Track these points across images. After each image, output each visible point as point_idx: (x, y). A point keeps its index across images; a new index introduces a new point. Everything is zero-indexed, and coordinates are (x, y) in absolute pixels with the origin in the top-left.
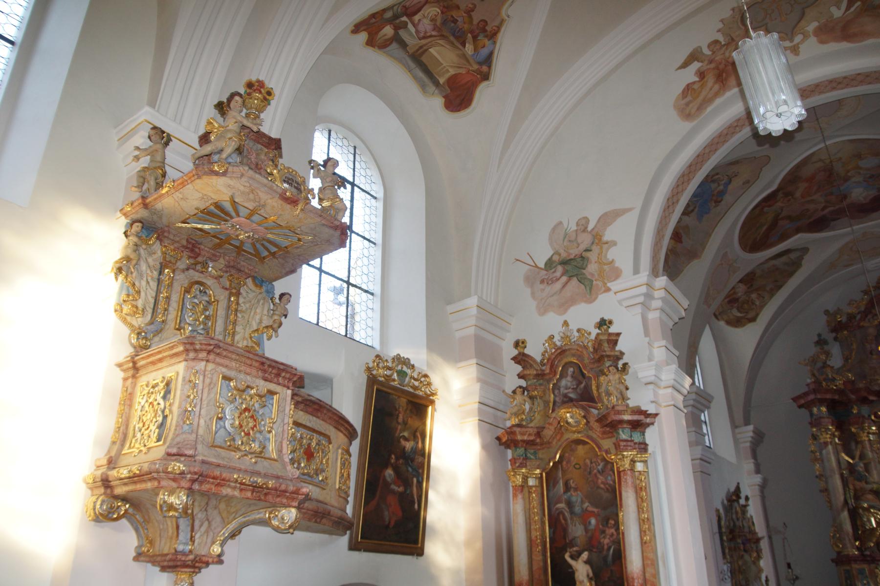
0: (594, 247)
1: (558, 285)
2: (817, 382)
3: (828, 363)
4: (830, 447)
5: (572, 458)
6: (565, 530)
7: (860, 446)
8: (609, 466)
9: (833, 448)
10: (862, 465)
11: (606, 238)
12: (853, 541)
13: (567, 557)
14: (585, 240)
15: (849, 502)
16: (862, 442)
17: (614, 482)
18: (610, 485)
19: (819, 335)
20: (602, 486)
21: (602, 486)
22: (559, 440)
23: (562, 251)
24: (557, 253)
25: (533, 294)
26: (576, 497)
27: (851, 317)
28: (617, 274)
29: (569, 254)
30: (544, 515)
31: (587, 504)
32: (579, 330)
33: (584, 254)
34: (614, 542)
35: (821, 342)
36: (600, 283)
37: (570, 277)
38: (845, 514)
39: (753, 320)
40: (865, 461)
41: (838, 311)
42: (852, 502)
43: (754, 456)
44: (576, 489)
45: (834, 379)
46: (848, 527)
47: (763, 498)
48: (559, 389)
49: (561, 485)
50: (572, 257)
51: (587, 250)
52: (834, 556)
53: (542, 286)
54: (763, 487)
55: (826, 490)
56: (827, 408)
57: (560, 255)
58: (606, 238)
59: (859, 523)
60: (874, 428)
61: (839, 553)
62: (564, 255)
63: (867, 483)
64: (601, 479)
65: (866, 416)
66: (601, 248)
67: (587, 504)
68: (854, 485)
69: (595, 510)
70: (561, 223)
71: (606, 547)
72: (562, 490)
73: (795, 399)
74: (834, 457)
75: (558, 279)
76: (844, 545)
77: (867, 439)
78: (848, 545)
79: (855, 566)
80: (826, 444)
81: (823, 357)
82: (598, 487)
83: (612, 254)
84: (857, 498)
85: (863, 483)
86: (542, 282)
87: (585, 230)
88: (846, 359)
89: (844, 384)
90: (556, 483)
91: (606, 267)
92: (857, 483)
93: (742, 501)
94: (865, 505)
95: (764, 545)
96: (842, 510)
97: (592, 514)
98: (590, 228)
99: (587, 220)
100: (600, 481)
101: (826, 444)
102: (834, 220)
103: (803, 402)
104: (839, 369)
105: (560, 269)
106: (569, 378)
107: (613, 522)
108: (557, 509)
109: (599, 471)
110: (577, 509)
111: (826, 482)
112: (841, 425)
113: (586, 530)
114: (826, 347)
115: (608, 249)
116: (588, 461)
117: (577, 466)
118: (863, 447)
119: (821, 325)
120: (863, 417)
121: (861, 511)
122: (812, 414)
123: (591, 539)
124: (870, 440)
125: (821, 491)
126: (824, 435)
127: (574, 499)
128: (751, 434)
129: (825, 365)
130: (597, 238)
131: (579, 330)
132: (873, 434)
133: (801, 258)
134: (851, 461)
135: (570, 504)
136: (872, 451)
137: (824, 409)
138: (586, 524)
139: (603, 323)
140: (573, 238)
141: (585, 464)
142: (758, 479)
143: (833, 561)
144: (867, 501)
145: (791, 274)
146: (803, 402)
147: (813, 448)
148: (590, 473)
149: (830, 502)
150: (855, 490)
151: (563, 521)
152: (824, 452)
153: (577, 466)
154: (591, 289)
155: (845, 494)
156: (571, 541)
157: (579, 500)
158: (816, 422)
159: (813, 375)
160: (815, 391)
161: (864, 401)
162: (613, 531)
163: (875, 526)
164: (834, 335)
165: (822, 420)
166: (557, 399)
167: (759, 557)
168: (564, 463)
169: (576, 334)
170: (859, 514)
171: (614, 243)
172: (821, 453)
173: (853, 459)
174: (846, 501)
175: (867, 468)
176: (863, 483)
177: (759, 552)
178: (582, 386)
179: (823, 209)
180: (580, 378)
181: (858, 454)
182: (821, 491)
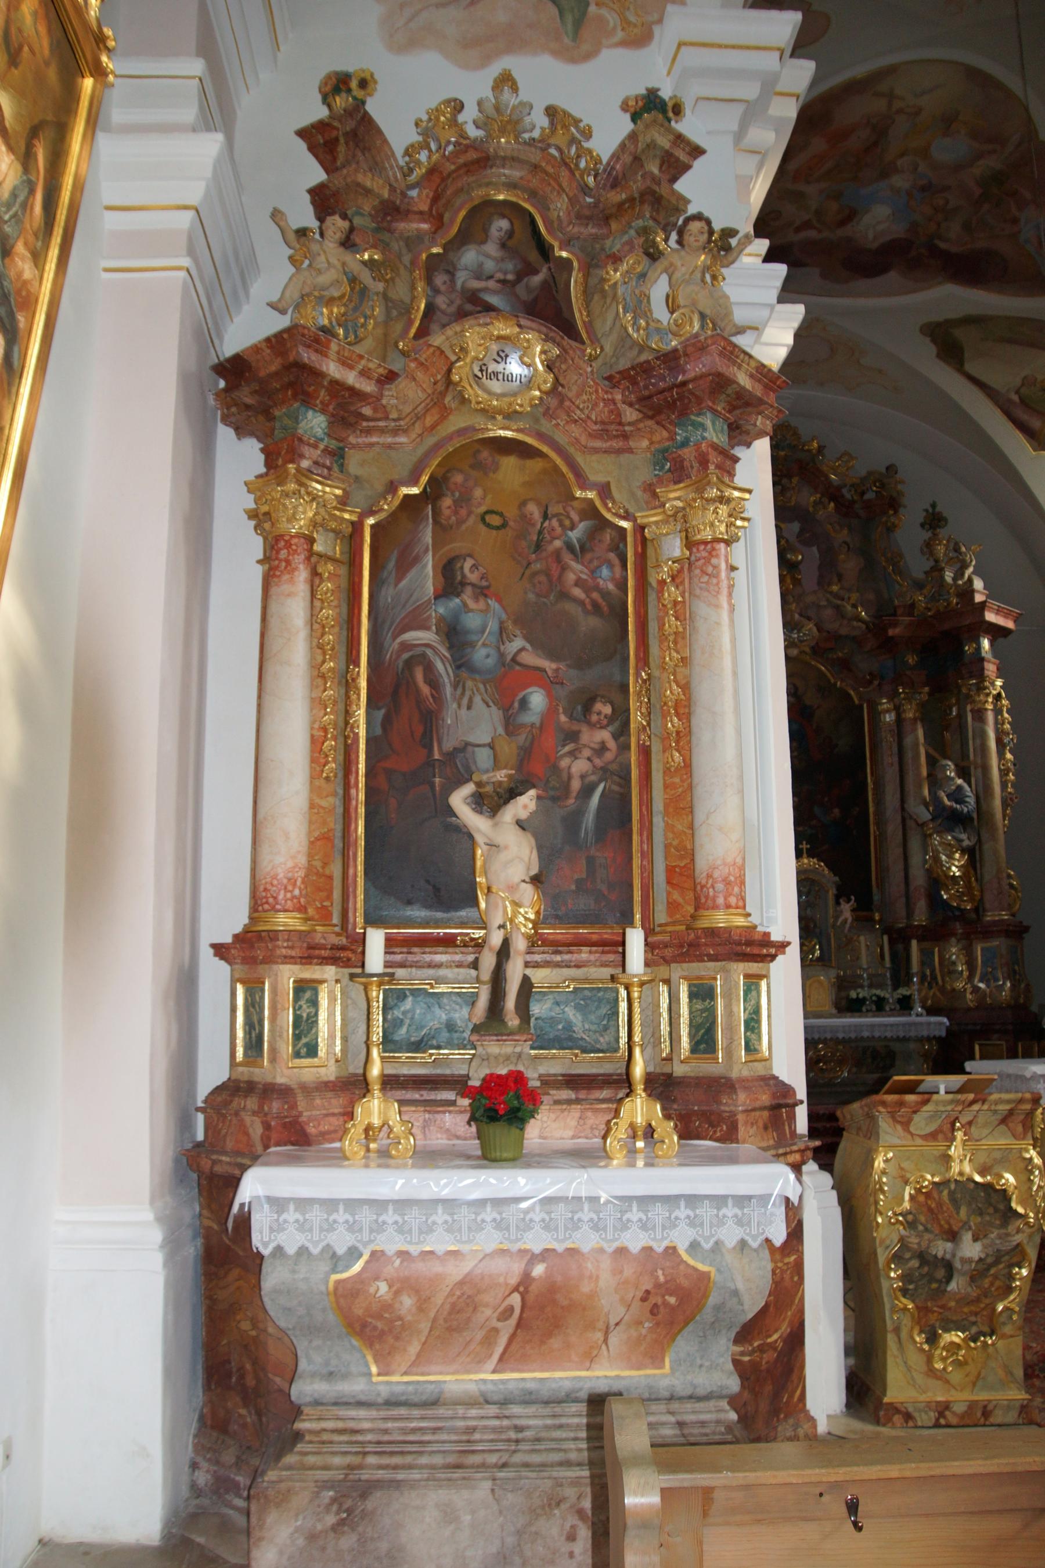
5: (478, 493)
6: (429, 720)
8: (608, 536)
13: (459, 800)
17: (623, 586)
18: (605, 594)
20: (578, 592)
21: (578, 592)
22: (433, 427)
26: (481, 618)
30: (353, 659)
31: (518, 643)
32: (551, 112)
34: (605, 772)
44: (482, 592)
48: (451, 273)
49: (426, 575)
64: (576, 570)
67: (518, 643)
69: (549, 666)
71: (576, 785)
72: (430, 589)
82: (564, 595)
90: (407, 562)
97: (537, 676)
100: (571, 577)
106: (491, 248)
107: (607, 710)
108: (405, 647)
109: (570, 547)
110: (482, 655)
113: (511, 726)
116: (534, 510)
117: (495, 520)
123: (526, 754)
127: (472, 621)
131: (551, 112)
135: (454, 635)
138: (510, 707)
139: (651, 108)
141: (525, 519)
148: (538, 546)
151: (425, 690)
153: (495, 520)
154: (578, 24)
156: (451, 756)
157: (493, 625)
162: (605, 735)
166: (441, 301)
168: (447, 502)
169: (543, 121)
178: (537, 279)
179: (798, 230)
180: (534, 256)
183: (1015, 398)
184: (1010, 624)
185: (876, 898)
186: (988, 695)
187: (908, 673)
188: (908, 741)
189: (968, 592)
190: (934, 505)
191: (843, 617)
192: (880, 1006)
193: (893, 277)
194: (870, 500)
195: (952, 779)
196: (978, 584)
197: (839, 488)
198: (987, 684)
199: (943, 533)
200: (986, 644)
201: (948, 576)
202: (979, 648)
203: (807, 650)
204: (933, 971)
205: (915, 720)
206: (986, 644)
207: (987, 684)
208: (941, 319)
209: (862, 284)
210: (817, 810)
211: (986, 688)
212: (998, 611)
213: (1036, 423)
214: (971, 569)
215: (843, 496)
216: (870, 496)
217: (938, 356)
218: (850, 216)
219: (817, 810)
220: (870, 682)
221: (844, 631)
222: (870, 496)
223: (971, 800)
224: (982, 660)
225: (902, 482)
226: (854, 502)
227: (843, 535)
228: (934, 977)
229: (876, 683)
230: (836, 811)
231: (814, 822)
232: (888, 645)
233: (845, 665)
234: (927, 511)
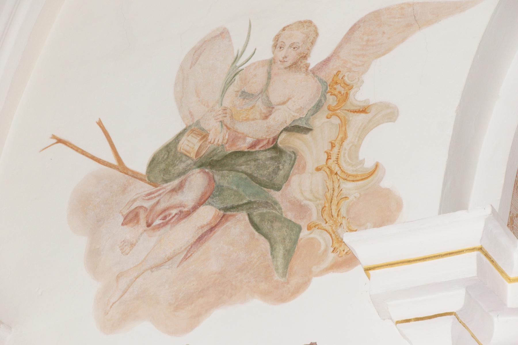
0: (319, 122)
1: (184, 232)
11: (360, 96)
14: (295, 95)
23: (212, 125)
24: (195, 129)
25: (93, 256)
28: (385, 210)
29: (236, 137)
33: (287, 141)
36: (322, 238)
37: (228, 210)
50: (243, 146)
51: (295, 129)
53: (129, 233)
57: (204, 136)
58: (360, 96)
62: (217, 136)
66: (344, 123)
70: (223, 34)
75: (185, 215)
83: (374, 147)
86: (131, 218)
87: (298, 64)
91: (348, 187)
98: (315, 59)
99: (309, 29)
105: (197, 182)
115: (365, 131)
130: (335, 92)
140: (256, 85)
171: (389, 113)
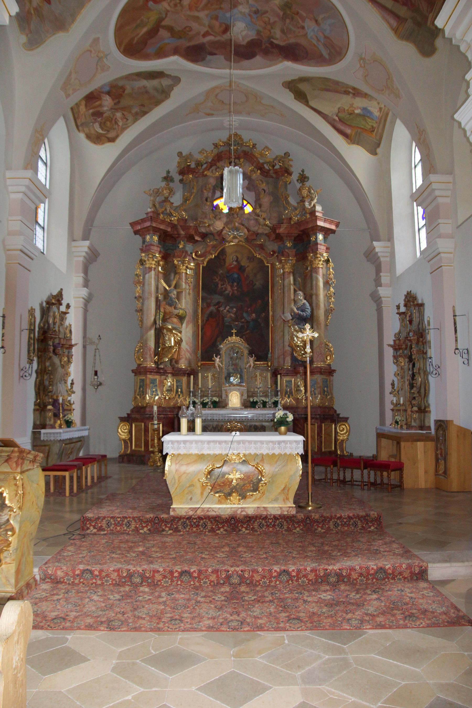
2: (156, 213)
3: (169, 199)
4: (153, 272)
7: (177, 276)
9: (155, 275)
10: (175, 292)
12: (153, 356)
15: (158, 322)
16: (180, 274)
19: (168, 172)
27: (199, 164)
35: (168, 179)
38: (152, 332)
39: (112, 140)
40: (179, 290)
41: (190, 155)
42: (159, 323)
43: (86, 271)
45: (171, 215)
46: (152, 344)
47: (86, 311)
52: (135, 367)
54: (87, 301)
55: (141, 311)
56: (159, 238)
59: (161, 341)
60: (192, 264)
61: (139, 365)
63: (175, 308)
65: (189, 253)
68: (164, 308)
73: (132, 225)
74: (153, 281)
76: (145, 359)
77: (185, 271)
78: (149, 359)
79: (150, 376)
80: (150, 269)
81: (166, 192)
84: (165, 320)
85: (173, 308)
88: (186, 200)
89: (178, 220)
92: (167, 307)
93: (63, 308)
94: (170, 327)
95: (77, 352)
96: (150, 329)
101: (150, 269)
102: (212, 54)
103: (139, 229)
104: (177, 207)
111: (143, 304)
112: (166, 257)
114: (171, 185)
118: (180, 278)
119: (173, 166)
120: (187, 252)
121: (165, 331)
122: (144, 241)
124: (186, 273)
125: (137, 311)
126: (151, 261)
128: (86, 249)
129: (166, 200)
132: (191, 269)
133: (171, 88)
134: (167, 288)
136: (186, 283)
137: (156, 238)
142: (84, 292)
143: (133, 371)
144: (173, 323)
145: (158, 103)
146: (139, 229)
147: (138, 272)
149: (142, 321)
150: (165, 313)
152: (147, 276)
155: (156, 316)
158: (146, 249)
159: (154, 205)
160: (151, 219)
161: (190, 239)
163: (173, 345)
164: (181, 177)
165: (152, 247)
167: (69, 362)
170: (163, 333)
172: (144, 278)
173: (169, 287)
174: (155, 322)
175: (178, 297)
176: (173, 308)
177: (70, 357)
179: (204, 36)
181: (174, 283)
182: (137, 311)
183: (337, 118)
184: (333, 227)
185: (270, 355)
186: (320, 260)
187: (286, 250)
188: (286, 282)
189: (313, 212)
190: (303, 171)
191: (259, 224)
192: (264, 404)
193: (258, 59)
194: (276, 169)
195: (301, 300)
196: (319, 208)
197: (263, 164)
198: (318, 255)
199: (307, 184)
200: (320, 237)
201: (307, 204)
202: (316, 239)
203: (242, 239)
204: (291, 390)
205: (290, 273)
206: (320, 237)
207: (318, 255)
208: (290, 80)
209: (246, 63)
210: (245, 315)
211: (318, 258)
212: (325, 221)
213: (348, 131)
214: (315, 201)
215: (264, 167)
216: (277, 167)
217: (295, 98)
218: (227, 29)
219: (245, 315)
220: (273, 255)
221: (260, 231)
222: (277, 167)
223: (309, 311)
224: (317, 244)
225: (292, 160)
226: (269, 170)
227: (264, 186)
228: (291, 393)
229: (276, 255)
230: (254, 315)
231: (243, 320)
232: (279, 238)
233: (262, 247)
234: (300, 174)
